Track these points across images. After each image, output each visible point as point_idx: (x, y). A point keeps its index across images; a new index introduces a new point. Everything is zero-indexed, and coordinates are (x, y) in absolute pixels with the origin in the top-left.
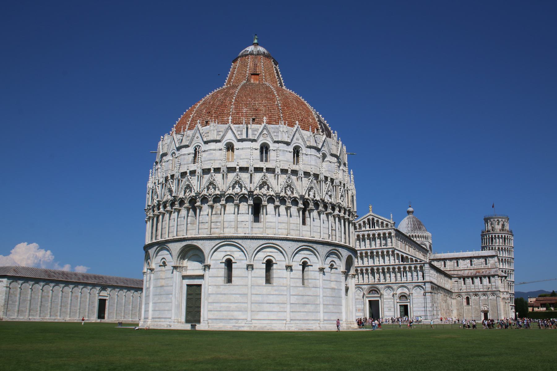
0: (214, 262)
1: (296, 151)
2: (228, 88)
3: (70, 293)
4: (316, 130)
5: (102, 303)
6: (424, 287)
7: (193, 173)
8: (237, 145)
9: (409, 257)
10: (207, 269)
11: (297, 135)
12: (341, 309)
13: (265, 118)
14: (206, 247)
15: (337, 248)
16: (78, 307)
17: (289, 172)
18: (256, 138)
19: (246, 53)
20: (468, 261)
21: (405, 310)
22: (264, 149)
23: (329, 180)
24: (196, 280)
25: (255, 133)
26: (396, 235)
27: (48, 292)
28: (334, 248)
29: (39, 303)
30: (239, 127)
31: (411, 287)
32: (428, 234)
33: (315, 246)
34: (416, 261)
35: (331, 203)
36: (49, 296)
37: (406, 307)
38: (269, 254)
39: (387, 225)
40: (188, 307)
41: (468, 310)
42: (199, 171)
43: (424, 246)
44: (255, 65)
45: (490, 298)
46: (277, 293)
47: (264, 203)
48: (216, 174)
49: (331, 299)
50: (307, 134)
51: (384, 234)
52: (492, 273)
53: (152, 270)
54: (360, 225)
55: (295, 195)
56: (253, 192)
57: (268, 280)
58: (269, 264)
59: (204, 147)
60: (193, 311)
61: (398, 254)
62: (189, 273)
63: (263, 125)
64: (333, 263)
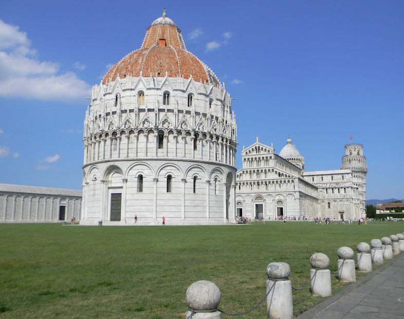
0: (130, 177)
1: (190, 97)
2: (142, 50)
3: (37, 203)
4: (205, 81)
5: (62, 209)
6: (294, 194)
7: (114, 113)
8: (146, 92)
9: (284, 174)
10: (125, 183)
11: (191, 85)
12: (223, 210)
13: (167, 72)
14: (123, 166)
15: (220, 167)
16: (44, 212)
17: (184, 112)
18: (160, 88)
19: (156, 23)
20: (330, 177)
21: (281, 212)
22: (166, 95)
23: (214, 118)
24: (118, 190)
25: (160, 83)
26: (275, 158)
27: (20, 202)
28: (217, 167)
29: (13, 210)
30: (148, 79)
31: (286, 195)
32: (303, 158)
33: (203, 165)
34: (289, 176)
35: (215, 135)
36: (20, 205)
37: (282, 209)
38: (169, 171)
39: (269, 151)
40: (112, 210)
41: (329, 212)
42: (118, 112)
43: (298, 166)
44: (163, 33)
45: (345, 203)
46: (175, 198)
47: (166, 134)
48: (131, 113)
49: (215, 202)
50: (199, 84)
51: (267, 157)
52: (347, 186)
53: (87, 183)
54: (250, 151)
55: (188, 129)
56: (158, 127)
57: (168, 189)
58: (169, 178)
59: (123, 94)
60: (116, 214)
61: (276, 172)
62: (113, 185)
63: (165, 77)
64: (217, 177)
